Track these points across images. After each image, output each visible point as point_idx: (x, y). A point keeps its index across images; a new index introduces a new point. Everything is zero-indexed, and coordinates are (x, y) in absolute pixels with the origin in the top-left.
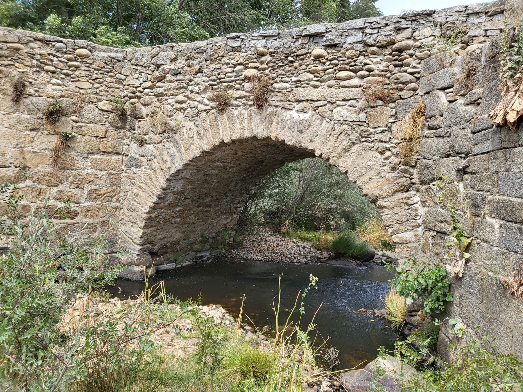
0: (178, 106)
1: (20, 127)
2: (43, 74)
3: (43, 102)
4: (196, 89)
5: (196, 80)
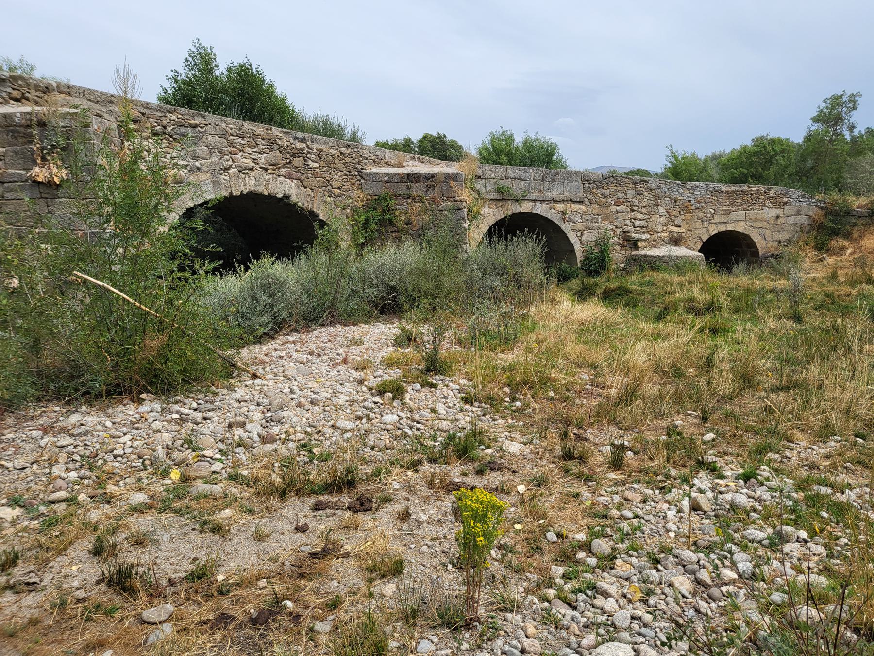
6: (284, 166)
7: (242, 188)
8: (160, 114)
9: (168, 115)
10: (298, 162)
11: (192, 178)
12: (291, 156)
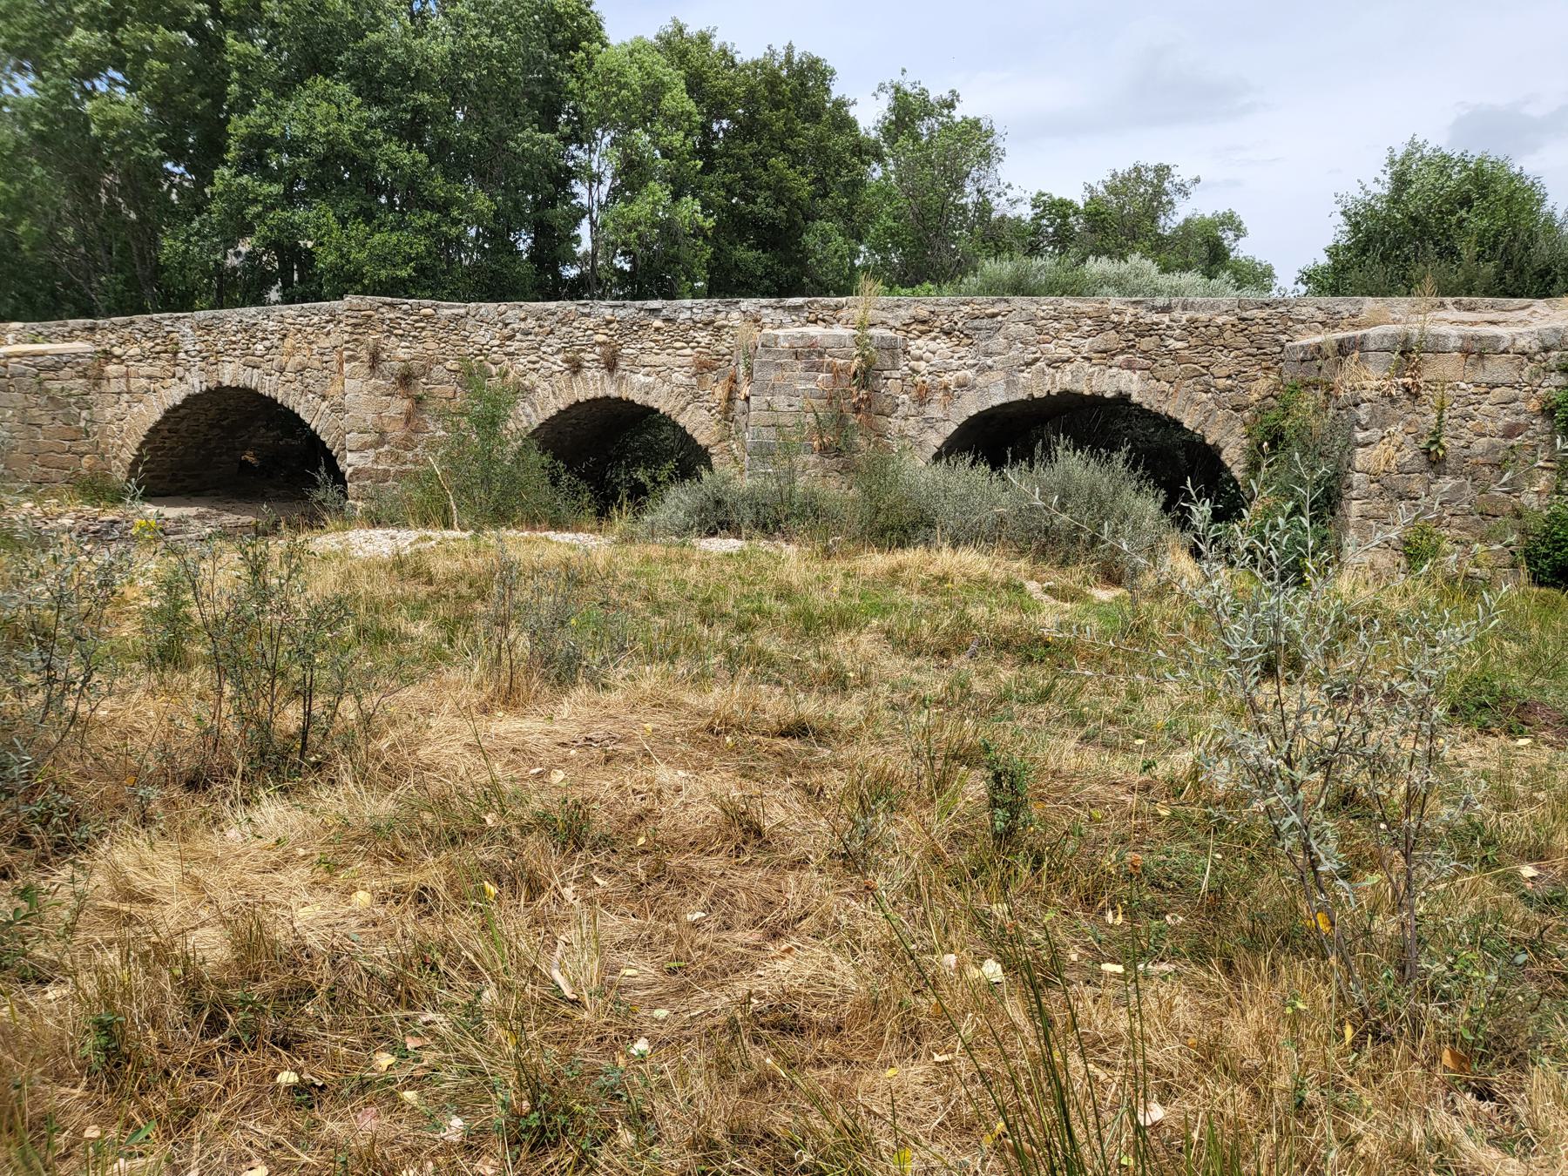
0: (531, 366)
1: (377, 393)
2: (393, 338)
3: (397, 365)
4: (549, 350)
5: (548, 341)
6: (1122, 351)
7: (1049, 387)
8: (951, 309)
9: (962, 308)
10: (1146, 343)
11: (981, 380)
12: (1137, 336)
